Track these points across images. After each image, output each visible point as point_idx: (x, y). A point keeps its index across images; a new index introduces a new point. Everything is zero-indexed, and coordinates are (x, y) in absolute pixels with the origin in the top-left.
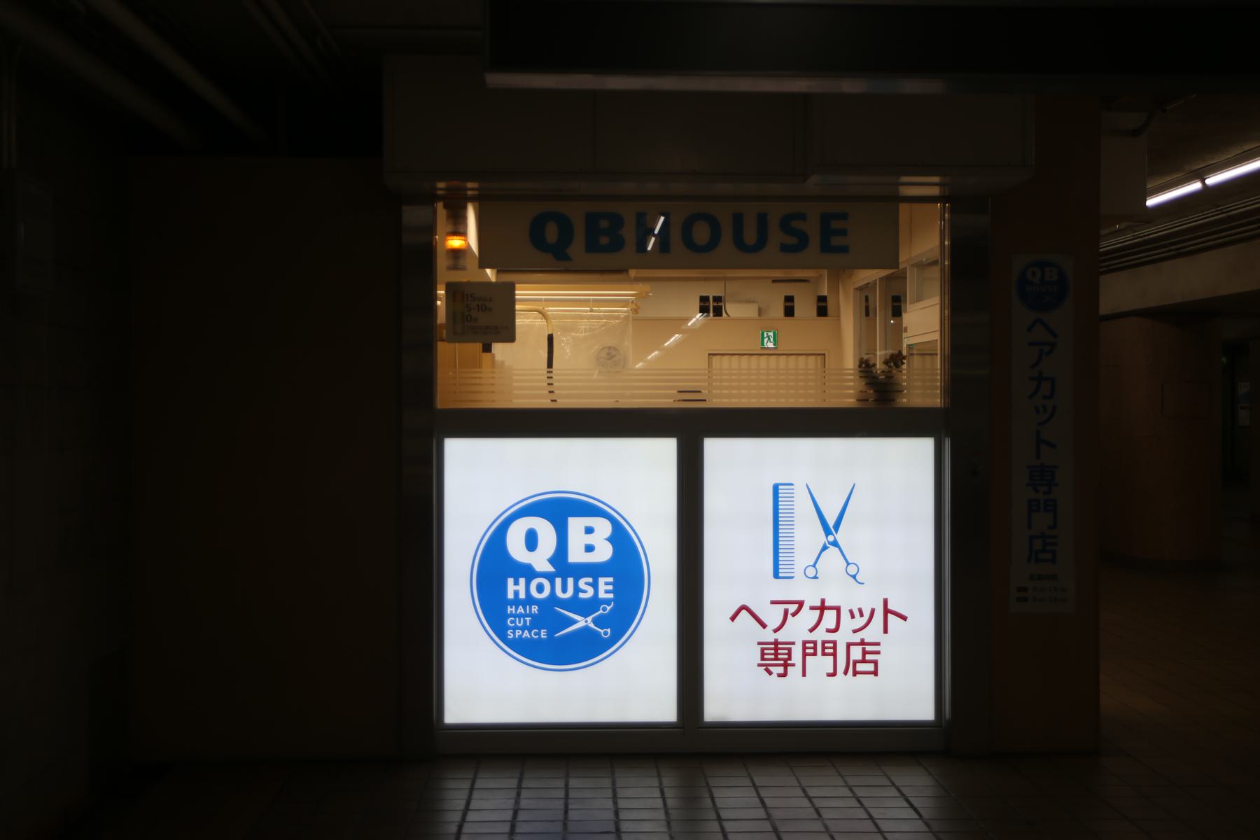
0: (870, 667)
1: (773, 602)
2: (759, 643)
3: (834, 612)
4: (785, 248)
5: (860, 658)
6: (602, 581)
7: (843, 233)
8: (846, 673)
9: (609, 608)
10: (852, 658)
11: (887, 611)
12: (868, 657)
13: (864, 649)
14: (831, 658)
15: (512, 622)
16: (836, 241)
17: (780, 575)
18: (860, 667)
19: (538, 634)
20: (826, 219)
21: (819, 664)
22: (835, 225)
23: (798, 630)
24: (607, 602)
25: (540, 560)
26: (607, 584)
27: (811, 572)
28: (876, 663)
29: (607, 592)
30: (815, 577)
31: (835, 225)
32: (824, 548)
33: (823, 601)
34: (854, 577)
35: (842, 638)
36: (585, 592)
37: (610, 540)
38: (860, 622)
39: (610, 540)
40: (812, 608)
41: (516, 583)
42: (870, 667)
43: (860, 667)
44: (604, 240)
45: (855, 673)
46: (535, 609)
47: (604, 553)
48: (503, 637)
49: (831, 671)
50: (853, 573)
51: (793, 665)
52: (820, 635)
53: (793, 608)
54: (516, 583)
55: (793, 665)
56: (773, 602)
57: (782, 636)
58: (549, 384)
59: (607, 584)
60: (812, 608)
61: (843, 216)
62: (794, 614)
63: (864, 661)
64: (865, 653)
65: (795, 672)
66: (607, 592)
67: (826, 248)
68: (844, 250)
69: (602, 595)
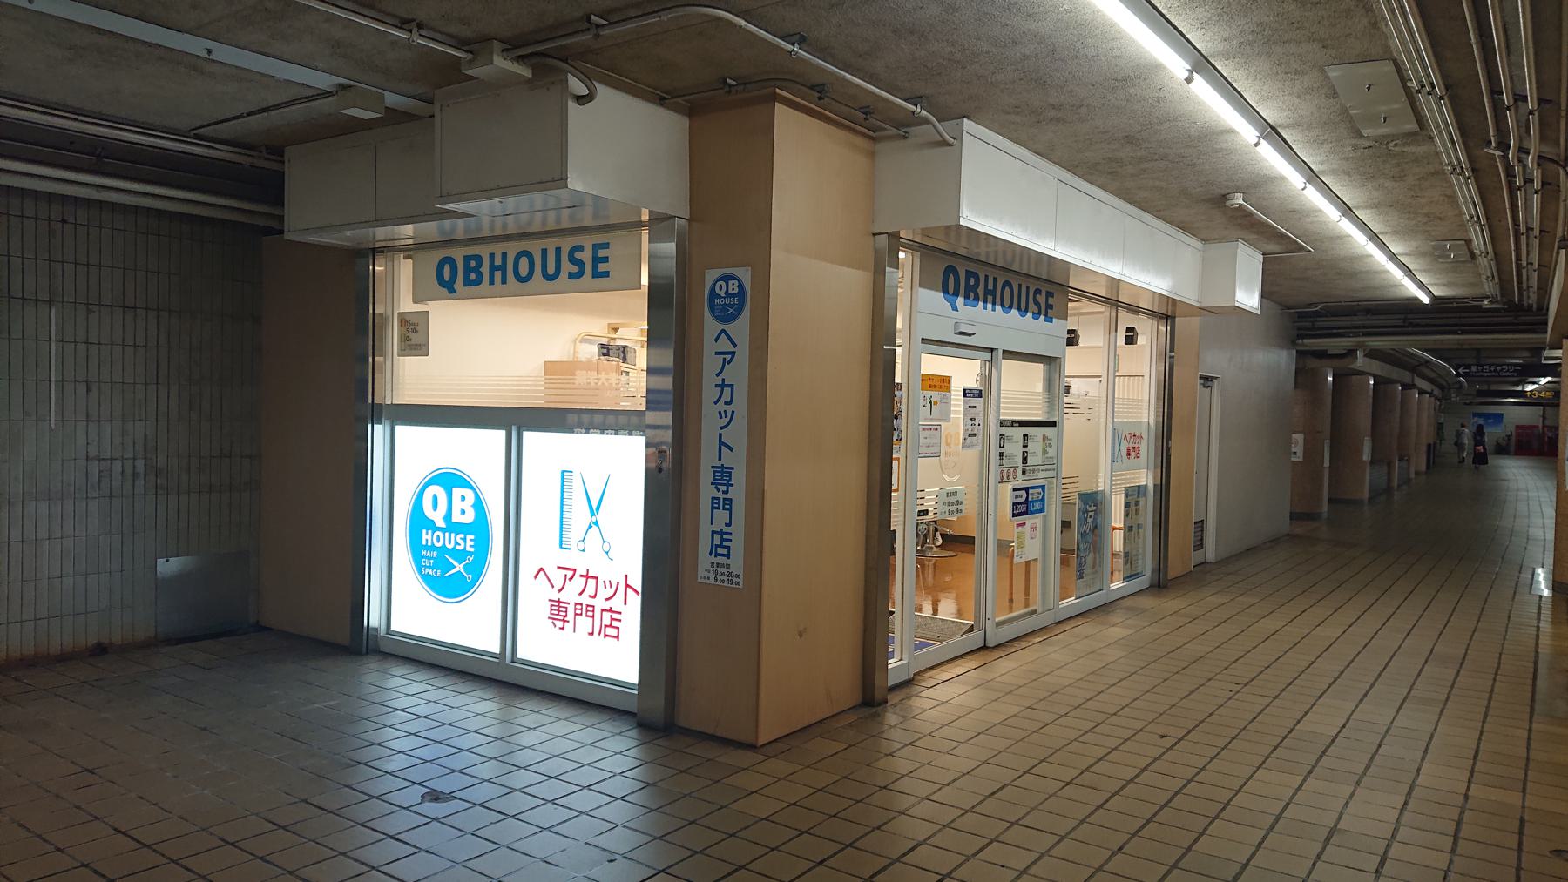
0: (725, 551)
1: (559, 568)
2: (550, 600)
3: (594, 581)
4: (572, 276)
5: (609, 624)
6: (469, 537)
7: (606, 259)
8: (600, 633)
9: (471, 559)
10: (715, 543)
11: (627, 586)
12: (614, 623)
13: (722, 537)
14: (591, 619)
15: (425, 562)
16: (602, 267)
17: (563, 546)
18: (720, 550)
19: (436, 573)
20: (596, 247)
21: (584, 623)
22: (602, 253)
23: (571, 594)
24: (471, 553)
25: (438, 518)
26: (471, 540)
27: (581, 546)
28: (728, 548)
29: (471, 546)
30: (584, 551)
31: (602, 253)
32: (590, 527)
33: (732, 485)
34: (607, 553)
35: (599, 603)
36: (460, 545)
37: (473, 506)
38: (610, 592)
39: (473, 506)
40: (582, 576)
41: (427, 534)
42: (725, 551)
43: (720, 550)
44: (473, 276)
45: (606, 636)
46: (435, 554)
47: (469, 517)
48: (420, 572)
49: (591, 631)
50: (607, 550)
51: (568, 621)
52: (585, 600)
53: (570, 574)
54: (427, 534)
55: (568, 621)
56: (559, 568)
57: (563, 597)
58: (605, 350)
59: (471, 540)
60: (582, 576)
61: (606, 246)
62: (571, 579)
63: (722, 546)
64: (723, 540)
65: (569, 626)
66: (471, 546)
67: (597, 274)
68: (606, 274)
69: (468, 549)
